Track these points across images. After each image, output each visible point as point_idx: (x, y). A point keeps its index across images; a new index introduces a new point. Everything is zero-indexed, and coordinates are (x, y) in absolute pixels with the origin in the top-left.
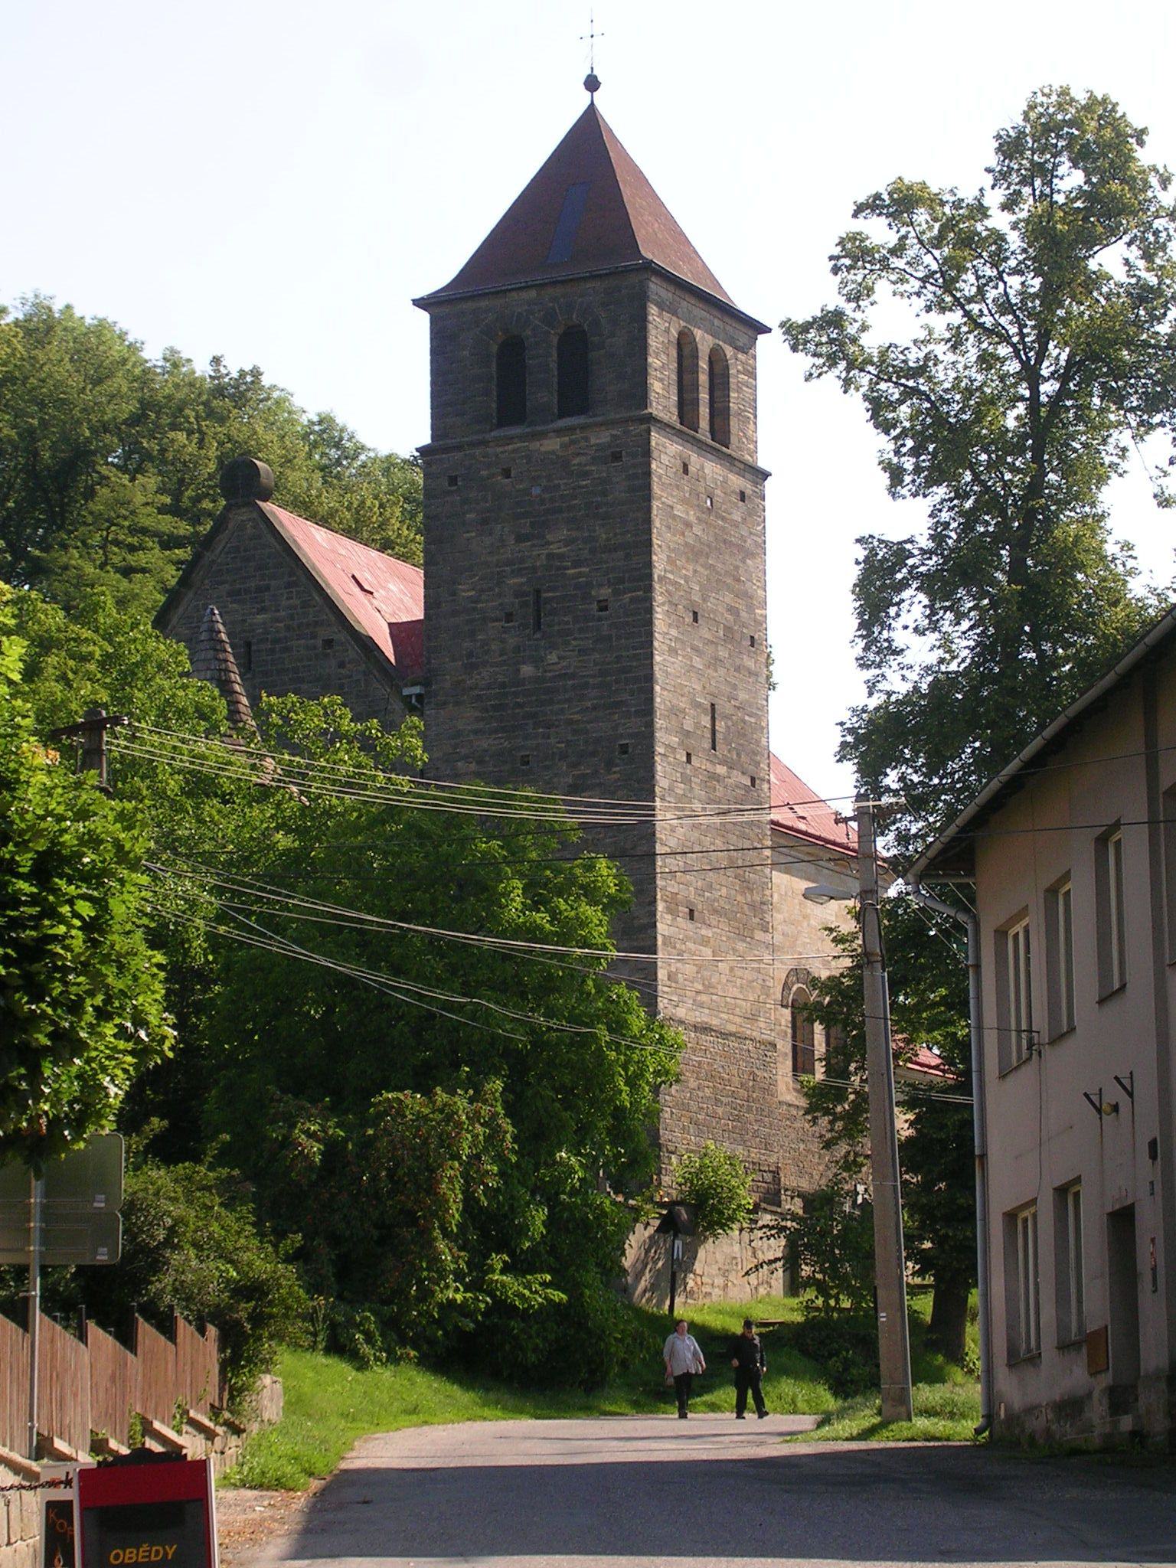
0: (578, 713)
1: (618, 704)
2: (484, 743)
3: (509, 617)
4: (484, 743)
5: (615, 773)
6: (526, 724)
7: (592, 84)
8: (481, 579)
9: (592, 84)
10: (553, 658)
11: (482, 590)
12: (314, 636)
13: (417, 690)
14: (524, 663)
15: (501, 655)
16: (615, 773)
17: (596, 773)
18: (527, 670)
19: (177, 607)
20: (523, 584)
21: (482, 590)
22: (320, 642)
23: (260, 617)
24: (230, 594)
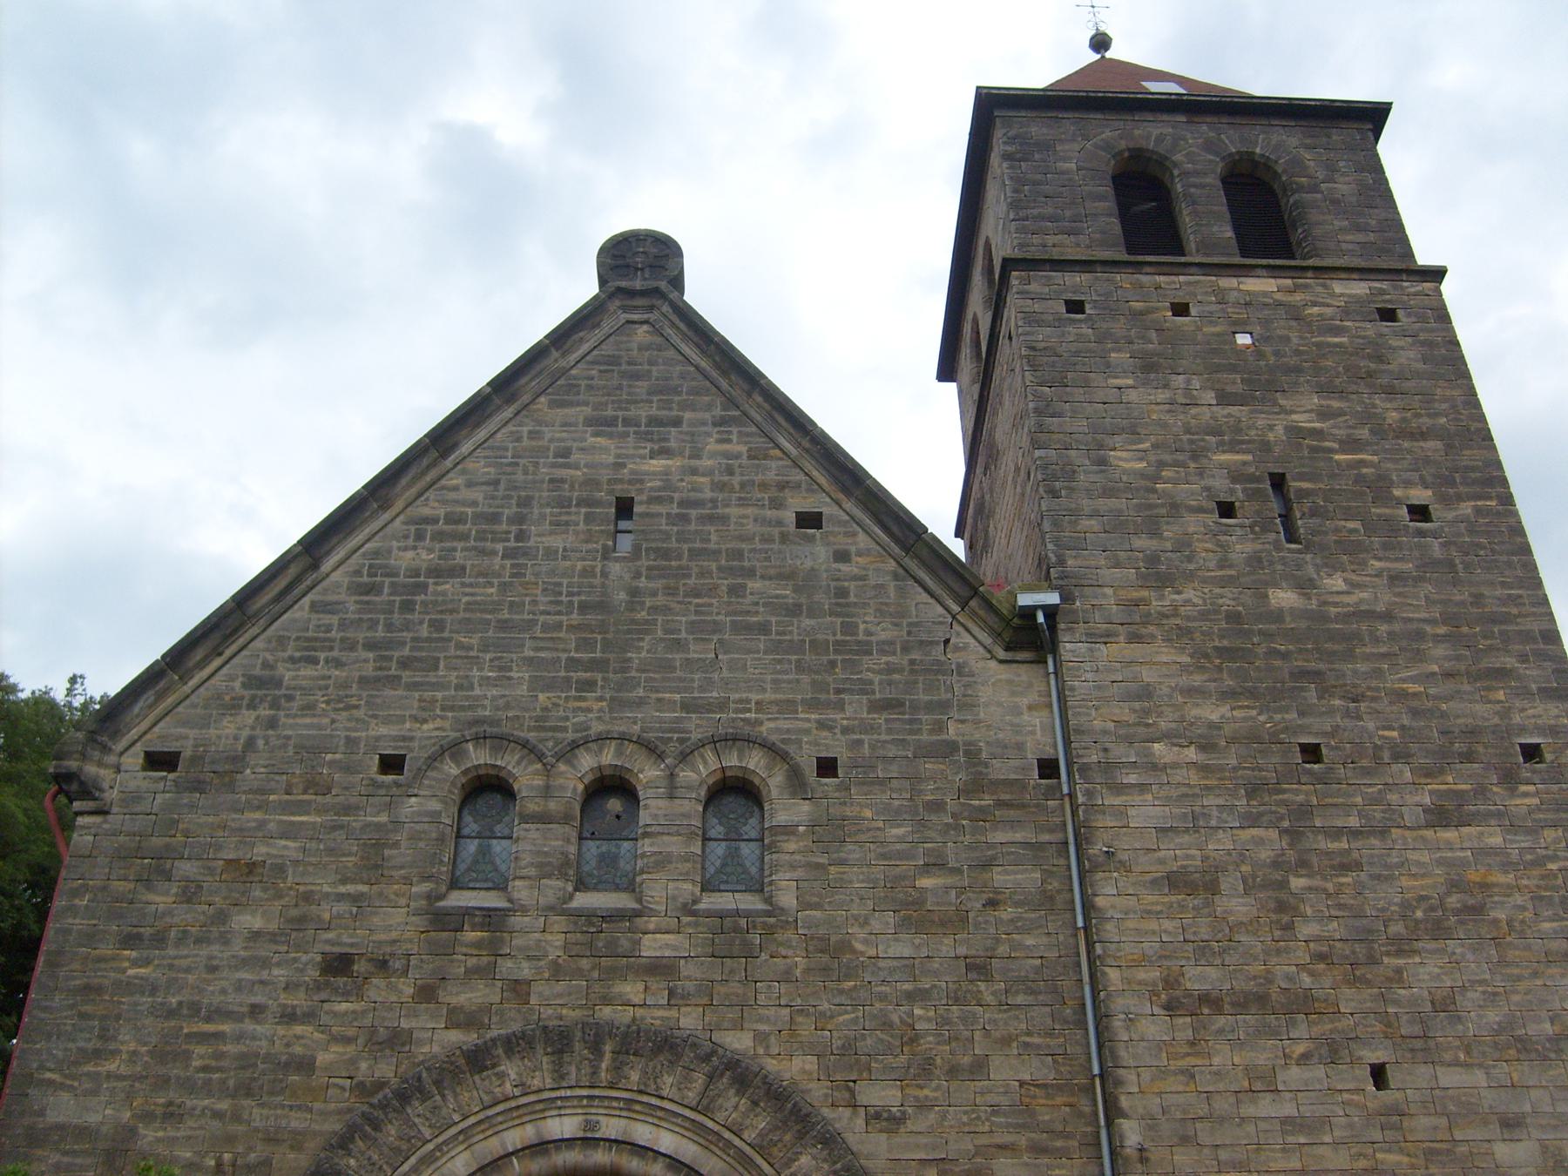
0: (1413, 679)
1: (1502, 674)
2: (1212, 712)
3: (1227, 510)
4: (1212, 712)
5: (1526, 795)
6: (1302, 689)
7: (1100, 42)
8: (1155, 446)
9: (1100, 42)
10: (1337, 582)
11: (1161, 464)
12: (777, 504)
13: (1053, 598)
14: (1276, 585)
15: (1221, 567)
16: (1526, 795)
17: (1481, 791)
18: (1283, 598)
19: (478, 425)
20: (1245, 463)
21: (1161, 464)
22: (790, 517)
23: (657, 464)
24: (589, 422)
